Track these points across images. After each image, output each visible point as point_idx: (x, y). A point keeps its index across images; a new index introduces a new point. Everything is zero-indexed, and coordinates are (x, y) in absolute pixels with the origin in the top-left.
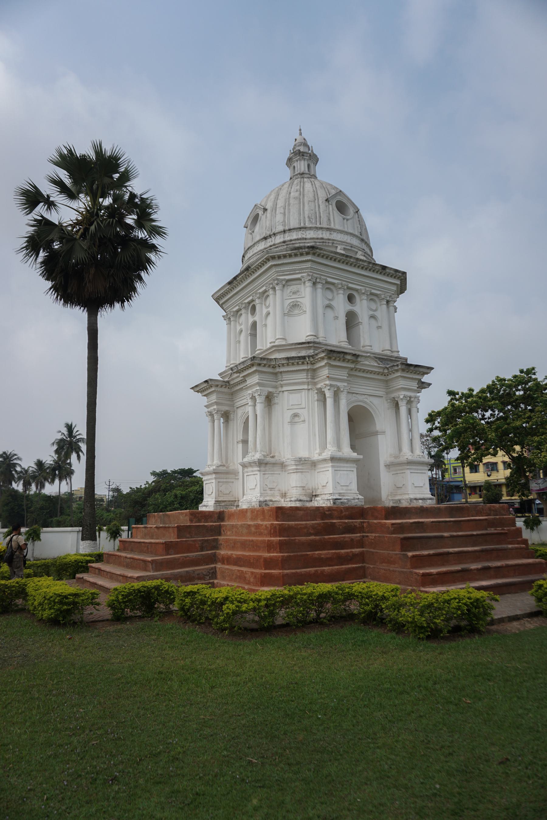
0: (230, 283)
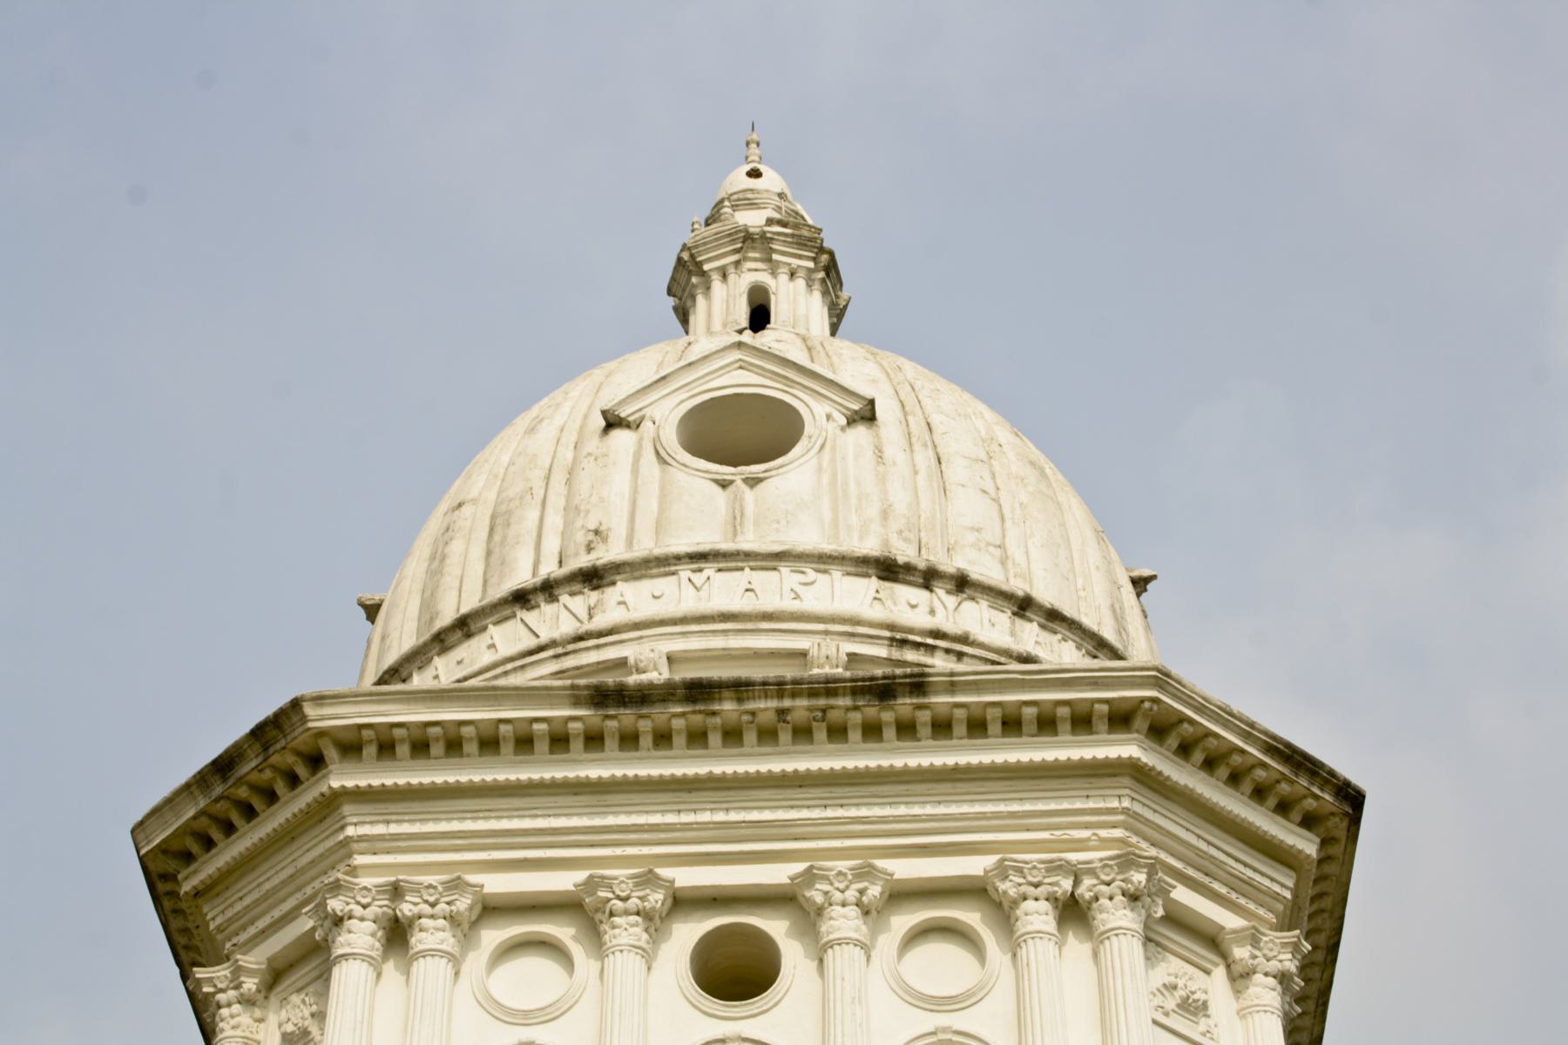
0: (605, 697)
